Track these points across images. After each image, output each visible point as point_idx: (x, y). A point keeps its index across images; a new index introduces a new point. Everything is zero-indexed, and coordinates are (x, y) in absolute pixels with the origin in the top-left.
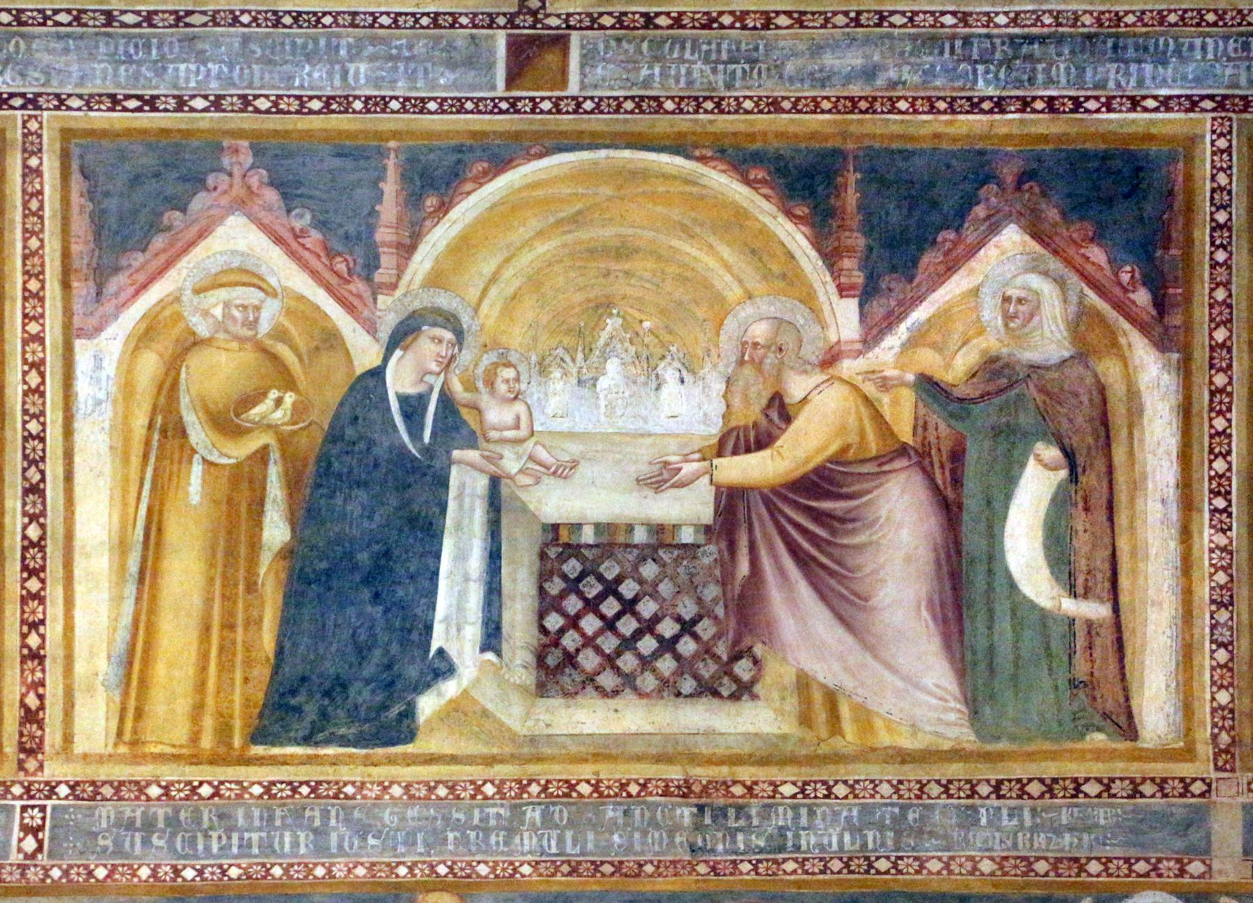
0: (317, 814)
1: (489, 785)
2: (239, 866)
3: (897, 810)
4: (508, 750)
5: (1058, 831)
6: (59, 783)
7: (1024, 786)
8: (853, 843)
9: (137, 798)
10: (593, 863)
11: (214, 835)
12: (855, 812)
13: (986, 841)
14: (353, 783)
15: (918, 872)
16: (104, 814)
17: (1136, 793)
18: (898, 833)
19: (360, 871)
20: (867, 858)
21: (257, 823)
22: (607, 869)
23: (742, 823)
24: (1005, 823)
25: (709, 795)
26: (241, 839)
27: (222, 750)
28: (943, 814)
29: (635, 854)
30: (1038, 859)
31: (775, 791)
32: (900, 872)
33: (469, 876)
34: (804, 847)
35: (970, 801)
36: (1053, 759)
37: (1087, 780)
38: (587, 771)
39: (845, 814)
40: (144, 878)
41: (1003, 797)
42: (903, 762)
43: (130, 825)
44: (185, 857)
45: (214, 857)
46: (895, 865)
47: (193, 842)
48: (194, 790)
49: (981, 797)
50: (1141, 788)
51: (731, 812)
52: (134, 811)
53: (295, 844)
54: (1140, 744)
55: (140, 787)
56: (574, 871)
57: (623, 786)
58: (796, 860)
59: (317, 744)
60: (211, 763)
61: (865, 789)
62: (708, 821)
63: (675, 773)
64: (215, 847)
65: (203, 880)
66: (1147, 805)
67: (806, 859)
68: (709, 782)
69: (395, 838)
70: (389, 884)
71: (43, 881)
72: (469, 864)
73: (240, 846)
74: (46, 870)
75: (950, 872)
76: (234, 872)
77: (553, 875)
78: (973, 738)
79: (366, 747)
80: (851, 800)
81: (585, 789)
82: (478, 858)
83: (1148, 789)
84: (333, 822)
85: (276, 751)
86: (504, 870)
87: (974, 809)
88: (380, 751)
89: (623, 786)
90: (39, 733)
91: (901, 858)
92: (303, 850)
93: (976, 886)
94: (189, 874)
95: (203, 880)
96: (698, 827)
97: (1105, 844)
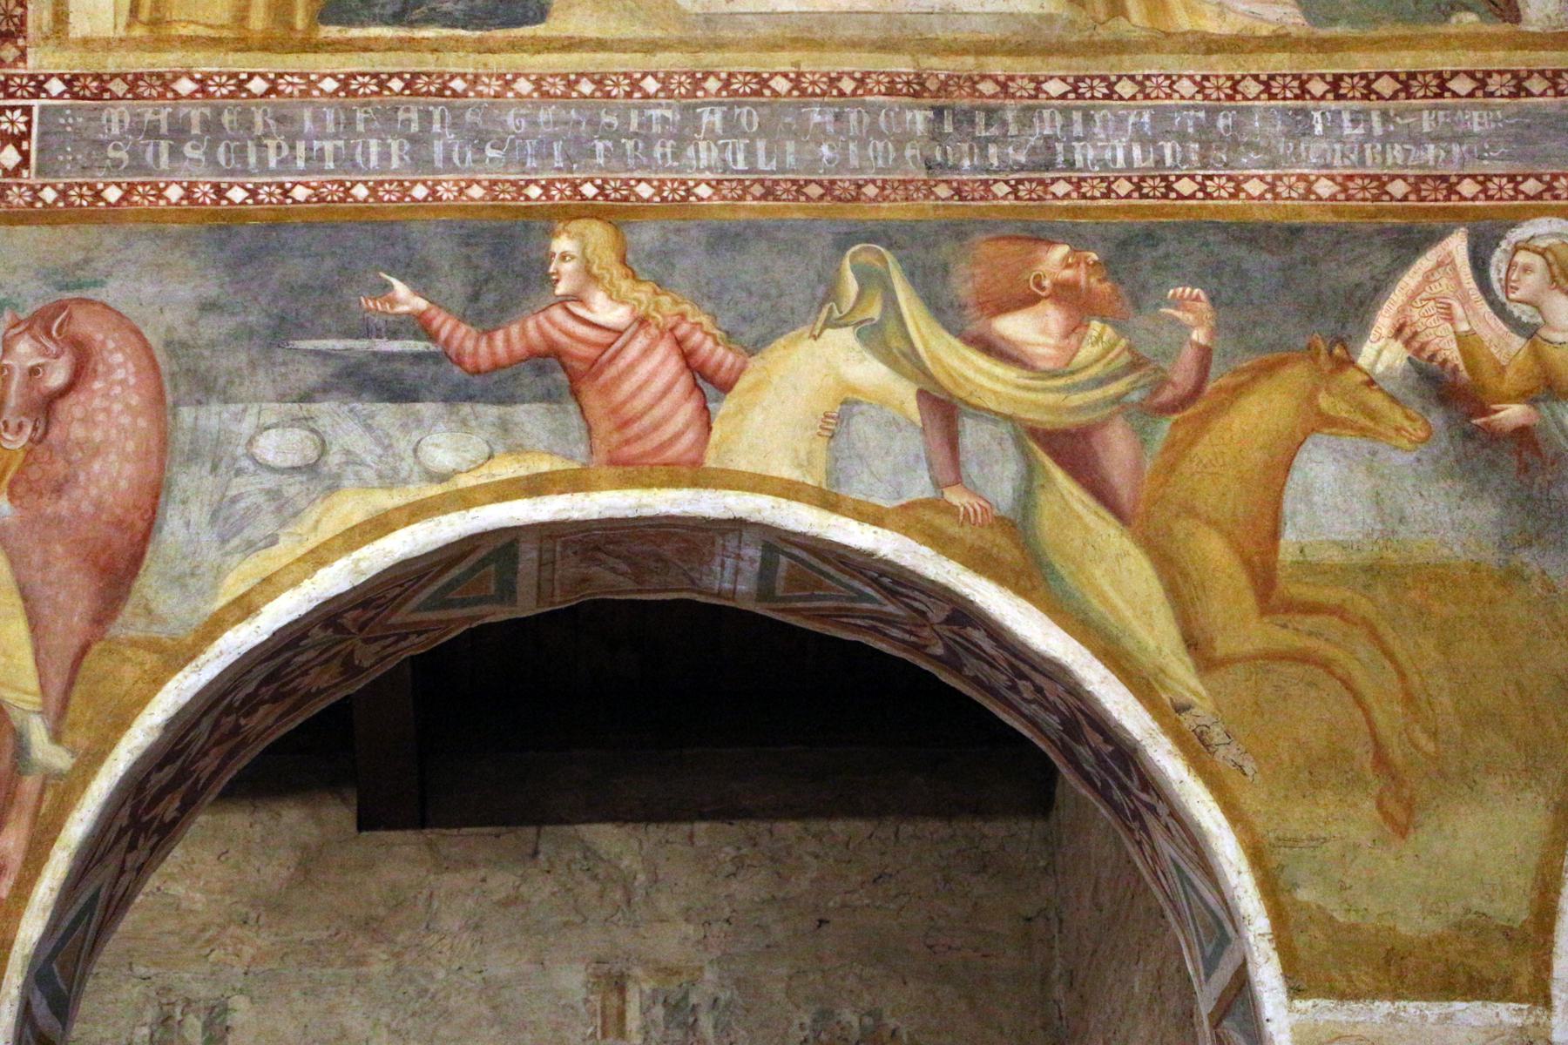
0: (414, 116)
1: (650, 79)
2: (307, 185)
3: (1202, 114)
4: (675, 33)
5: (1418, 141)
6: (49, 77)
7: (1370, 82)
8: (1144, 160)
9: (162, 96)
10: (794, 182)
11: (271, 143)
12: (1146, 118)
13: (1322, 155)
14: (463, 76)
15: (1233, 196)
16: (115, 119)
17: (1519, 90)
18: (1205, 146)
19: (476, 192)
20: (1164, 178)
21: (331, 128)
22: (815, 191)
23: (994, 131)
24: (1347, 132)
25: (949, 95)
26: (309, 149)
27: (279, 32)
28: (1264, 119)
29: (854, 171)
30: (1393, 178)
31: (1038, 89)
32: (1209, 196)
33: (626, 199)
34: (1079, 164)
35: (1300, 103)
36: (1407, 48)
37: (1455, 74)
38: (783, 61)
39: (1132, 119)
40: (174, 200)
41: (1344, 97)
42: (1209, 52)
43: (153, 132)
44: (232, 173)
45: (273, 173)
46: (1203, 187)
47: (242, 150)
48: (241, 85)
49: (1313, 98)
50: (1527, 84)
51: (980, 118)
52: (158, 113)
53: (385, 156)
54: (1522, 27)
55: (165, 82)
56: (769, 193)
57: (833, 81)
58: (1068, 180)
59: (412, 24)
60: (266, 48)
61: (1159, 86)
62: (948, 128)
63: (902, 65)
64: (273, 164)
65: (257, 202)
66: (1538, 106)
67: (1081, 179)
68: (949, 77)
69: (523, 148)
70: (518, 208)
71: (31, 205)
72: (626, 182)
73: (307, 160)
74: (35, 191)
75: (1277, 196)
76: (300, 193)
77: (741, 198)
78: (1301, 20)
79: (478, 27)
80: (1141, 102)
81: (781, 85)
82: (638, 175)
83: (1536, 85)
84: (436, 127)
85: (355, 33)
86: (674, 190)
87: (1306, 113)
88: (499, 34)
89: (833, 81)
90: (19, 11)
91: (1210, 178)
92: (395, 163)
93: (1313, 216)
94: (237, 195)
95: (257, 202)
96: (936, 136)
97: (1481, 158)
